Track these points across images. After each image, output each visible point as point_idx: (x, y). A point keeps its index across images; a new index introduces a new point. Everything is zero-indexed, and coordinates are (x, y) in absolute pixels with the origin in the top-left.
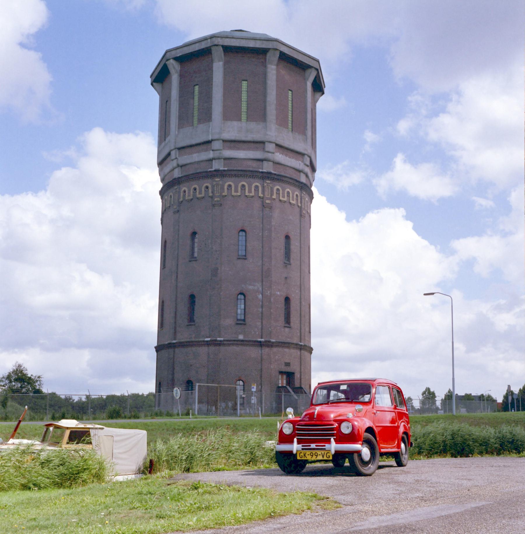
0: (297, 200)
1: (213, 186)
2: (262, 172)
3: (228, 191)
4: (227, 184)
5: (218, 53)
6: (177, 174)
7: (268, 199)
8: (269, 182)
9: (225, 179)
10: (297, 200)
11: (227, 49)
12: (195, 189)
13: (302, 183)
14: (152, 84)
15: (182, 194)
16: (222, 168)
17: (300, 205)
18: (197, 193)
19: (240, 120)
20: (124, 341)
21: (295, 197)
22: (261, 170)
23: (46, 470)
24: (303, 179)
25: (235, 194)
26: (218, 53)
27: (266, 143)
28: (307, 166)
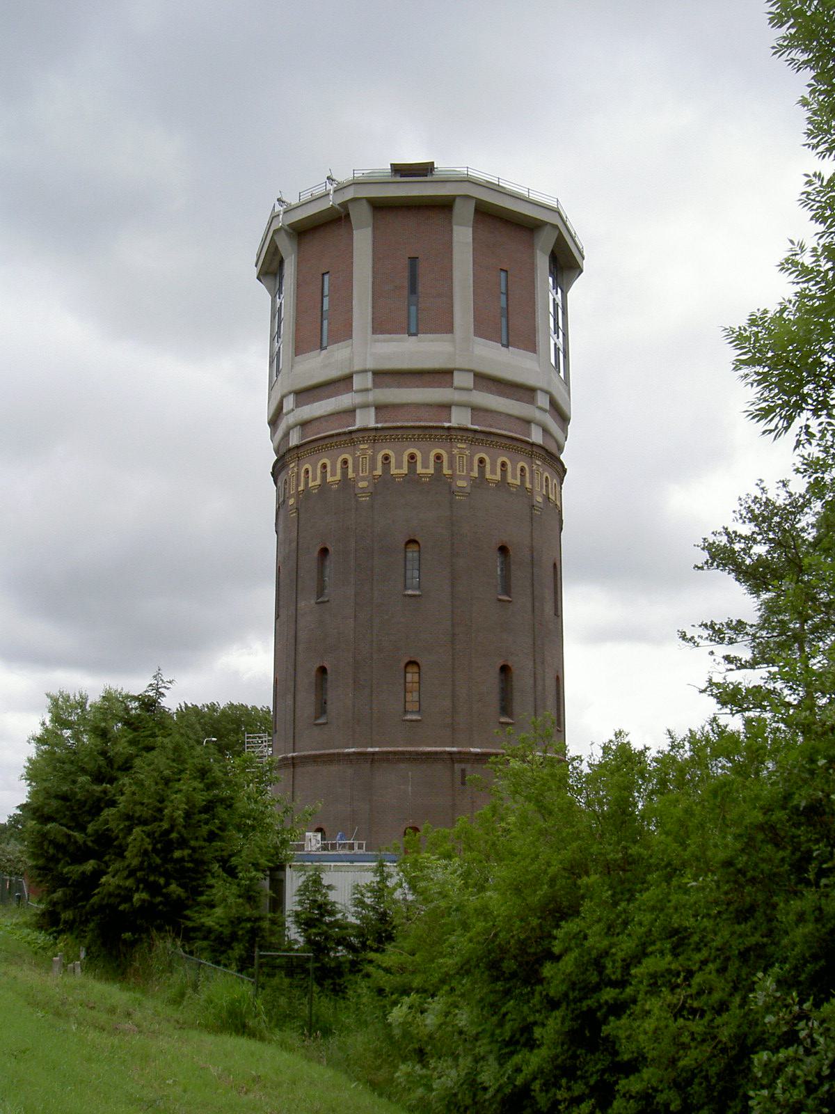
0: (523, 476)
1: (355, 460)
2: (449, 428)
3: (409, 468)
4: (382, 453)
5: (463, 212)
6: (294, 440)
7: (461, 478)
8: (464, 446)
9: (378, 446)
10: (523, 476)
11: (380, 207)
12: (324, 466)
13: (533, 444)
14: (258, 278)
15: (302, 475)
16: (372, 424)
17: (528, 485)
18: (329, 474)
19: (449, 329)
20: (599, 635)
21: (519, 472)
22: (447, 425)
23: (616, 777)
24: (536, 437)
25: (424, 471)
26: (463, 212)
27: (456, 373)
28: (544, 410)
